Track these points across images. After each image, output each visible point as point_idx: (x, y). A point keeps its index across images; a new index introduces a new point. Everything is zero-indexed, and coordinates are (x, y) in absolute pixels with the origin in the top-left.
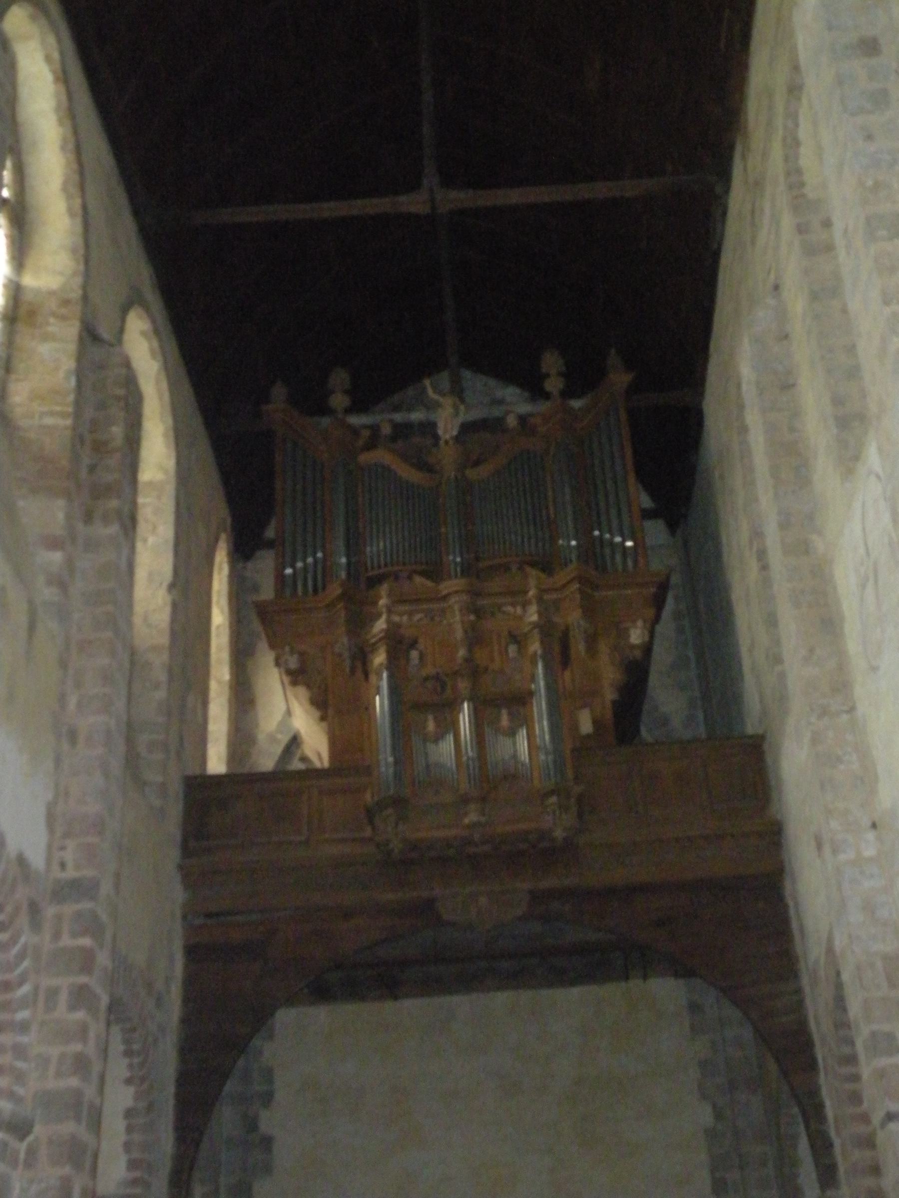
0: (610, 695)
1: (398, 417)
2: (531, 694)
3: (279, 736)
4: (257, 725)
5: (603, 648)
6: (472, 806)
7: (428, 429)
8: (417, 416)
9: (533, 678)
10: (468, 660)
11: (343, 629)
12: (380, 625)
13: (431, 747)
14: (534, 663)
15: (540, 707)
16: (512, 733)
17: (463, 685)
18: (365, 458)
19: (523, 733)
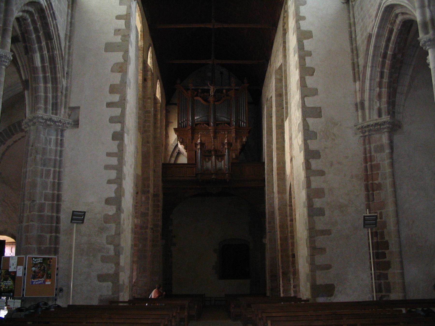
0: (239, 151)
1: (202, 88)
2: (225, 155)
3: (174, 144)
4: (169, 142)
5: (238, 141)
6: (214, 175)
7: (208, 91)
8: (206, 88)
9: (225, 152)
10: (214, 148)
11: (191, 135)
12: (199, 141)
13: (207, 163)
14: (226, 149)
15: (226, 157)
16: (221, 162)
17: (213, 153)
18: (195, 98)
19: (223, 162)
